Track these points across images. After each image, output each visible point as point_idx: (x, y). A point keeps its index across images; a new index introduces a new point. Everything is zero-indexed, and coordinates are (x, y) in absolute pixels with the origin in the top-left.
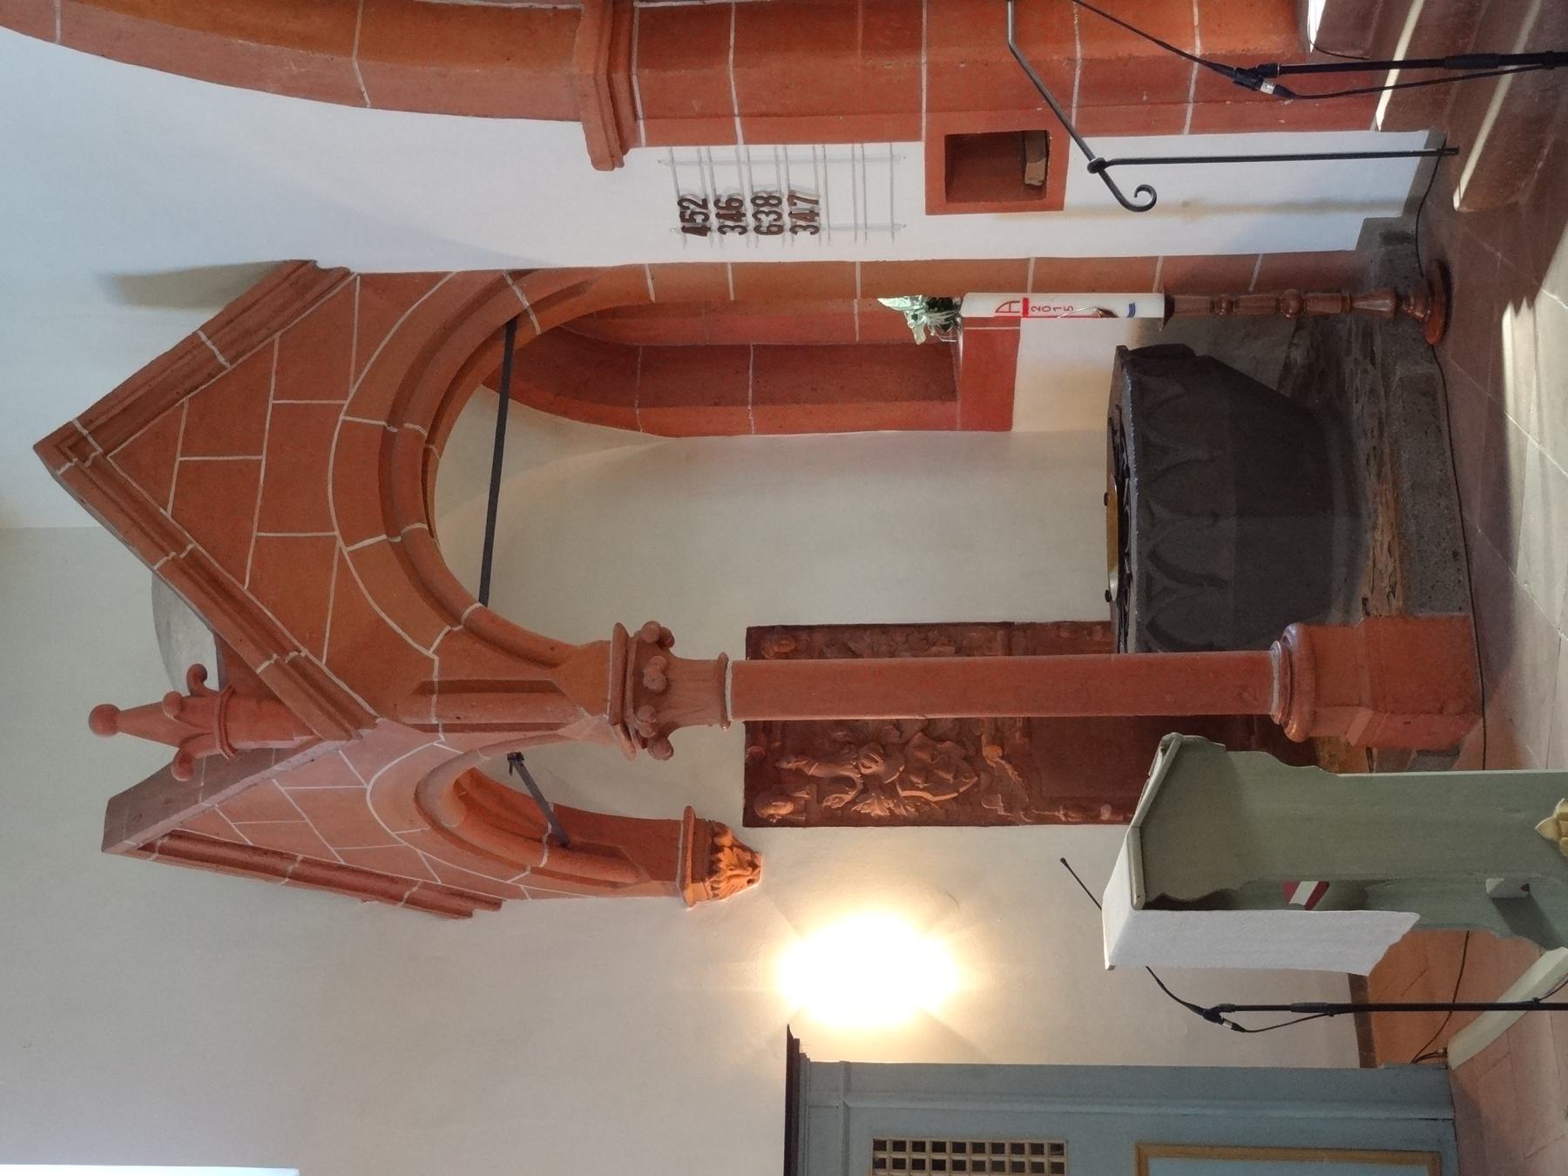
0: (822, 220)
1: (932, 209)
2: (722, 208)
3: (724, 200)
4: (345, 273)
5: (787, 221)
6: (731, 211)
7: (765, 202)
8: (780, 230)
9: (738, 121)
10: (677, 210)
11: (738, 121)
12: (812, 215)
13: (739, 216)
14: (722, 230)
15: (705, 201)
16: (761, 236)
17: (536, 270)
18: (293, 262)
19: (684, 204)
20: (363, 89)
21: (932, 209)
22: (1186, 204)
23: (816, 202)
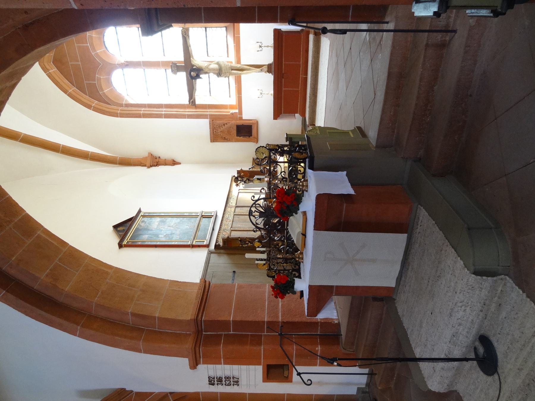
0: (240, 383)
1: (264, 381)
2: (217, 379)
3: (218, 377)
4: (132, 391)
5: (232, 383)
6: (220, 380)
7: (227, 378)
8: (230, 385)
9: (222, 359)
10: (208, 379)
11: (222, 359)
12: (237, 382)
13: (221, 381)
14: (217, 384)
15: (214, 377)
16: (226, 386)
17: (175, 392)
18: (121, 388)
19: (210, 378)
20: (142, 349)
21: (264, 381)
22: (319, 382)
23: (238, 379)
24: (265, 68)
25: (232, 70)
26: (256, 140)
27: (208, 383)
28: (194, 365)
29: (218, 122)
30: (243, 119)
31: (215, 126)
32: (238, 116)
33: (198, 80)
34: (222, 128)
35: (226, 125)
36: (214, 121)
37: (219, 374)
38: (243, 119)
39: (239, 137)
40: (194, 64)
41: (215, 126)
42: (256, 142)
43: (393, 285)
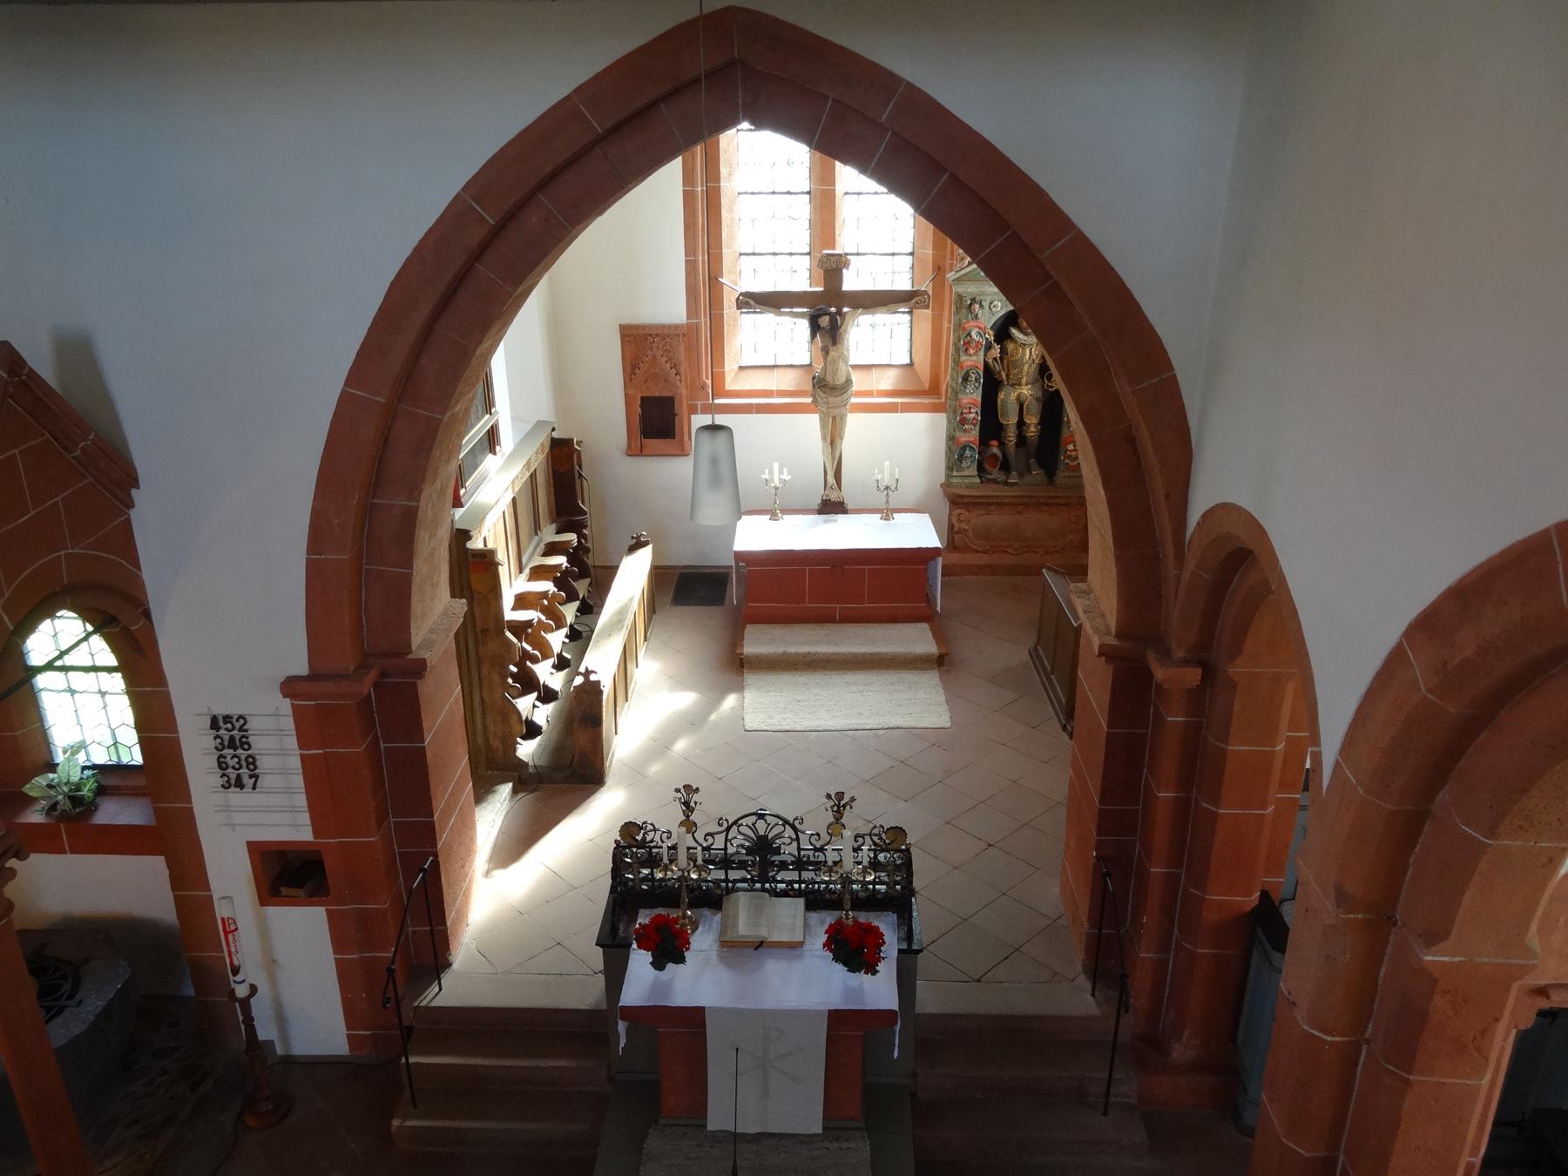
4: (130, 504)
7: (252, 762)
12: (239, 784)
13: (232, 744)
17: (152, 624)
22: (274, 961)
24: (834, 496)
25: (834, 418)
26: (635, 450)
27: (220, 711)
28: (290, 687)
29: (682, 348)
30: (693, 417)
31: (669, 340)
32: (699, 403)
33: (804, 325)
34: (666, 362)
35: (674, 371)
36: (685, 339)
37: (259, 744)
38: (693, 417)
39: (640, 403)
40: (846, 320)
41: (669, 340)
42: (629, 453)
43: (712, 1126)
